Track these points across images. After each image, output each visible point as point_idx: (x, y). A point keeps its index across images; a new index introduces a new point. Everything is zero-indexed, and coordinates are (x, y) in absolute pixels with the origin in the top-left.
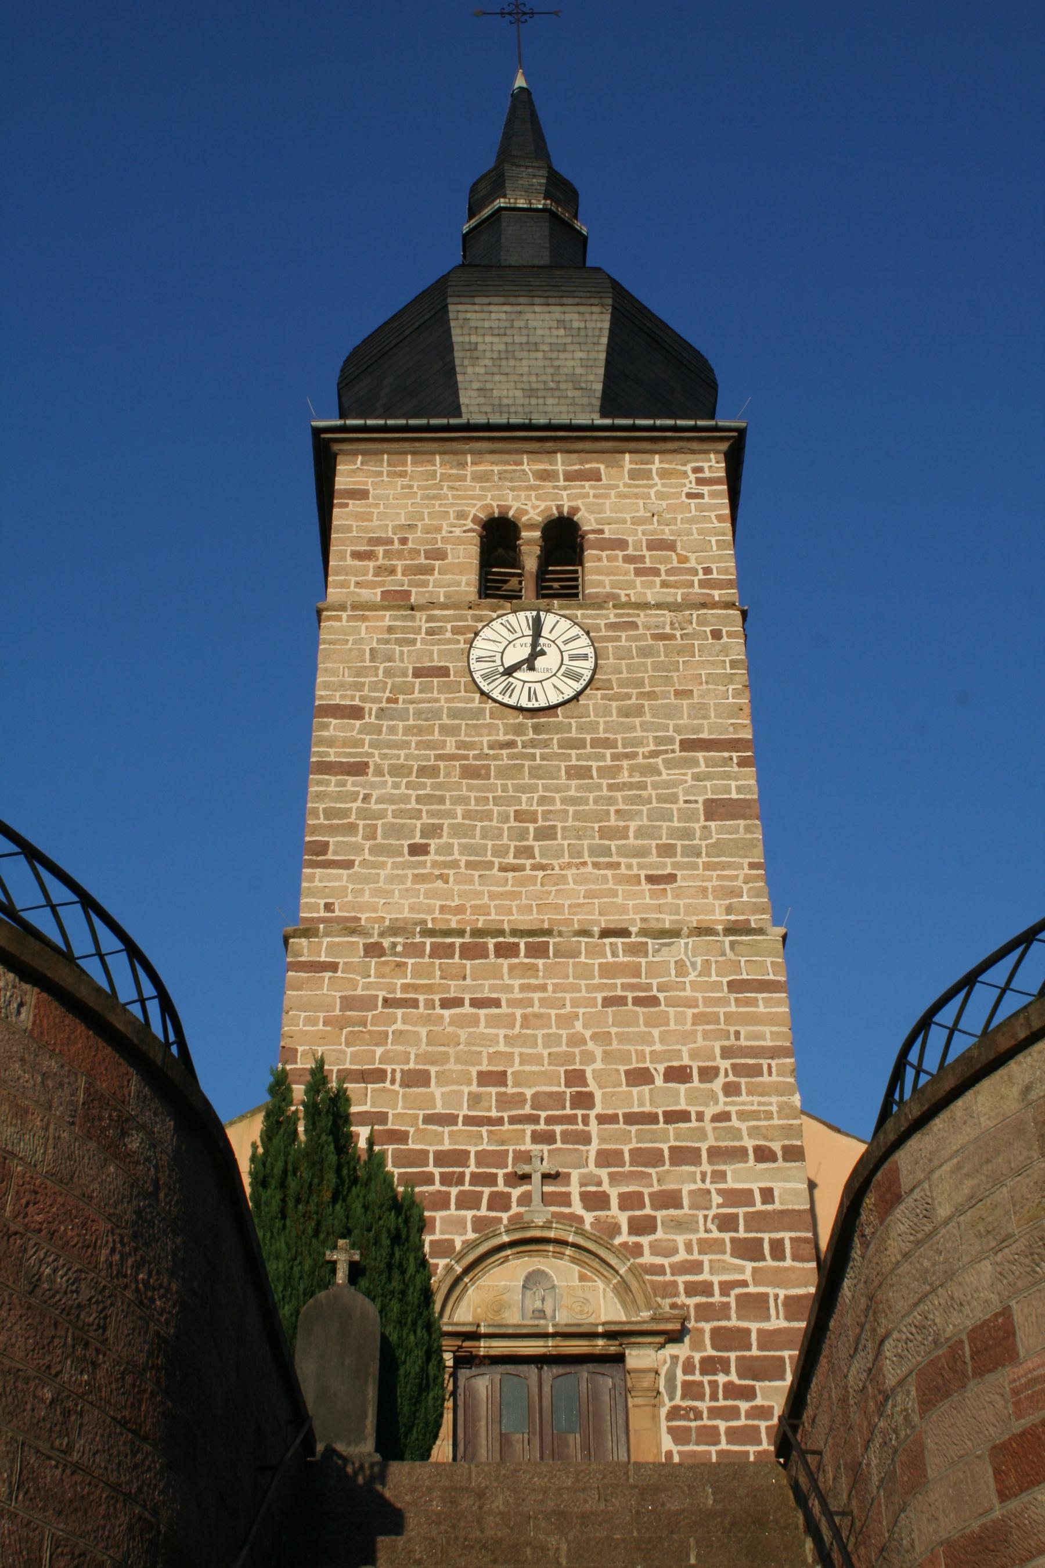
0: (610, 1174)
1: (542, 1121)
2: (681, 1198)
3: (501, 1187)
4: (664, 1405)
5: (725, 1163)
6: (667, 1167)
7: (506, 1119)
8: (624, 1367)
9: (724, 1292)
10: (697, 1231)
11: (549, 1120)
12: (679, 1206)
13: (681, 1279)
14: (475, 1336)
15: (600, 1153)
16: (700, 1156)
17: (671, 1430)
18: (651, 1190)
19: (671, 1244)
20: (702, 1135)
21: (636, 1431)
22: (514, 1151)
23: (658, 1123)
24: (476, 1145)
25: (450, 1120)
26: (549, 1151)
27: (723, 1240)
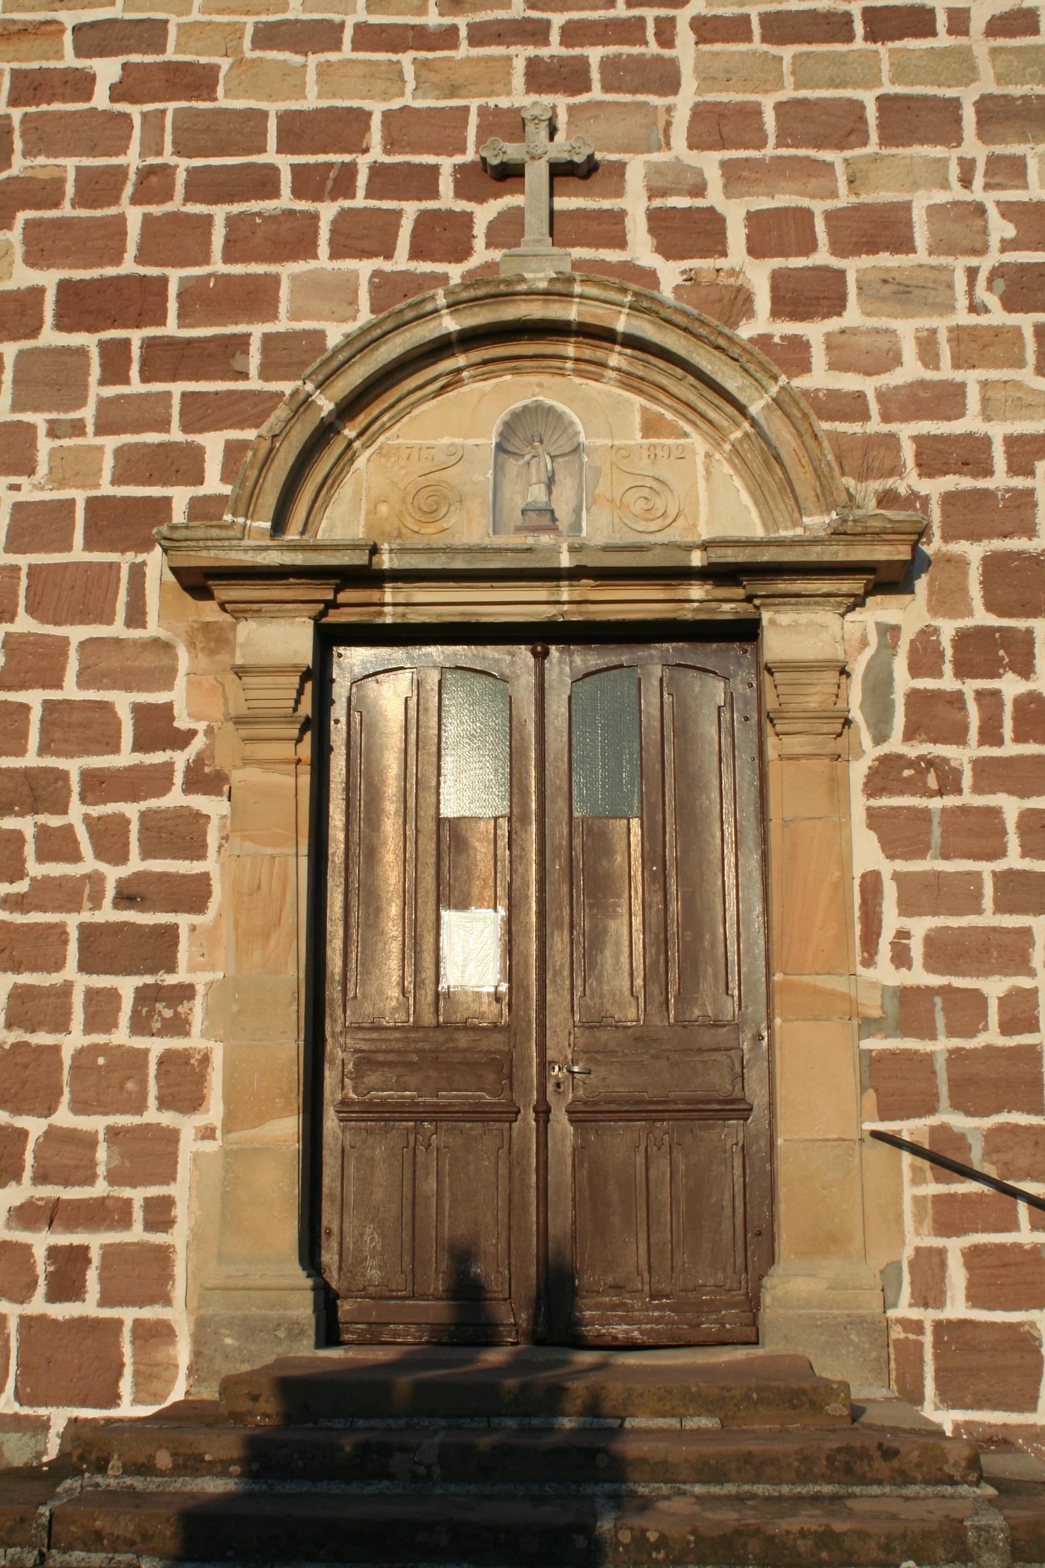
0: (724, 165)
1: (555, 36)
2: (909, 224)
3: (447, 199)
4: (860, 754)
5: (1023, 139)
6: (873, 147)
7: (463, 33)
8: (758, 652)
9: (1020, 466)
10: (950, 308)
11: (572, 34)
12: (904, 245)
13: (907, 431)
14: (368, 577)
15: (699, 113)
16: (958, 120)
17: (876, 819)
18: (831, 204)
19: (883, 342)
20: (965, 69)
21: (785, 823)
22: (483, 111)
23: (850, 38)
24: (385, 96)
25: (320, 36)
26: (571, 109)
27: (1017, 330)
